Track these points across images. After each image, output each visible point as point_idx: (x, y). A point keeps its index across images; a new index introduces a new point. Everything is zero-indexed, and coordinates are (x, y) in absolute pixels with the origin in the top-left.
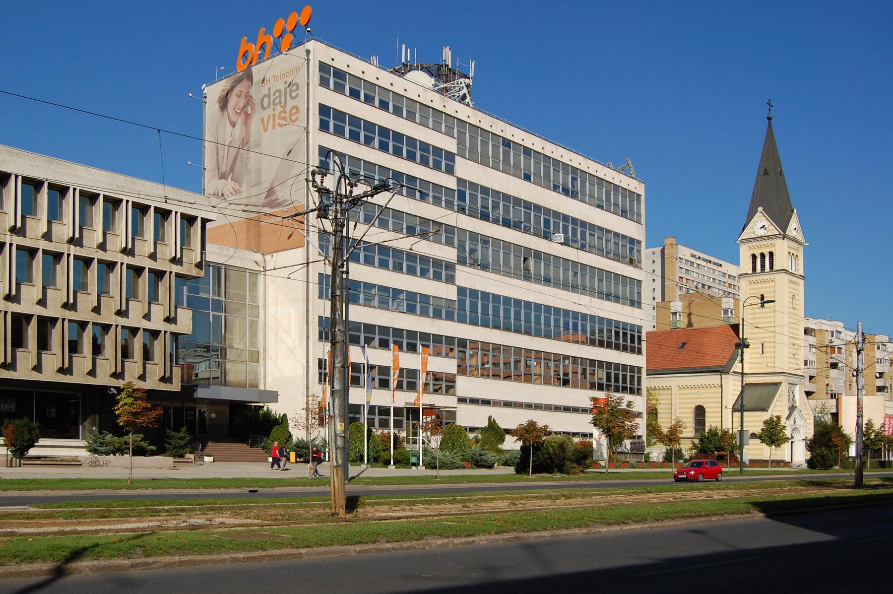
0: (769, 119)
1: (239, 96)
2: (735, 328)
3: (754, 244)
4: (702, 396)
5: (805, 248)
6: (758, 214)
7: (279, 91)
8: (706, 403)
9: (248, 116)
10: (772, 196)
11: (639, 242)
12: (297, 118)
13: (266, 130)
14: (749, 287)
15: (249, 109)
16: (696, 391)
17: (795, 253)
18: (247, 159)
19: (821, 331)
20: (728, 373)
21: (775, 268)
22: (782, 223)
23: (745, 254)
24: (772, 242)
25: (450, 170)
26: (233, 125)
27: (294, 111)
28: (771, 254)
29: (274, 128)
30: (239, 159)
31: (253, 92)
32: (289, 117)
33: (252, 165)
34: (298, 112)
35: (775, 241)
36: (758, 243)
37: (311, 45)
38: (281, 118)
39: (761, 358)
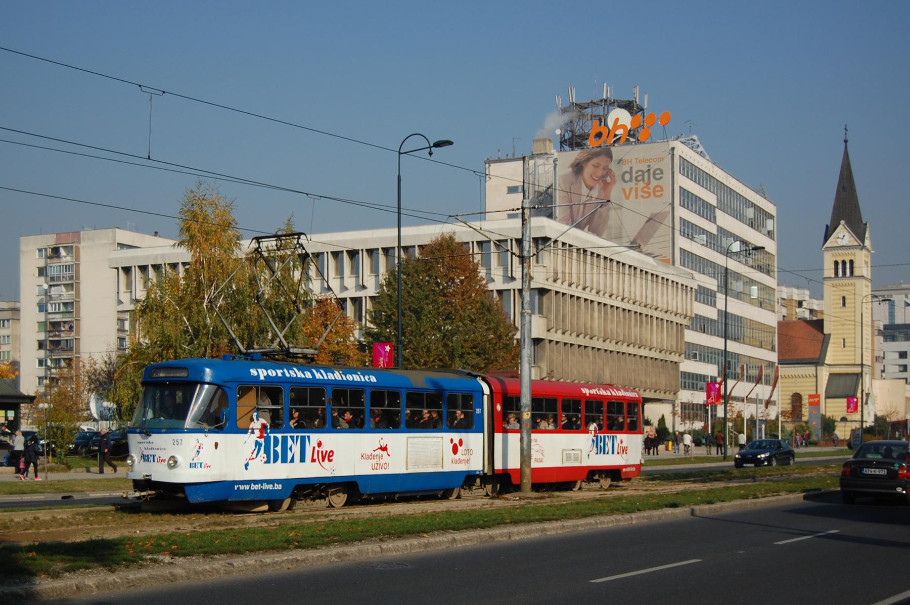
0: (846, 141)
1: (596, 166)
2: (819, 325)
3: (837, 252)
5: (872, 254)
6: (840, 227)
7: (642, 171)
9: (606, 186)
10: (847, 209)
13: (627, 198)
15: (608, 179)
18: (607, 216)
20: (822, 364)
21: (856, 273)
22: (862, 238)
23: (828, 260)
24: (853, 251)
25: (713, 219)
26: (591, 188)
27: (658, 189)
28: (852, 262)
29: (637, 197)
30: (597, 216)
31: (613, 166)
32: (658, 192)
34: (662, 190)
36: (840, 252)
37: (677, 144)
38: (643, 191)
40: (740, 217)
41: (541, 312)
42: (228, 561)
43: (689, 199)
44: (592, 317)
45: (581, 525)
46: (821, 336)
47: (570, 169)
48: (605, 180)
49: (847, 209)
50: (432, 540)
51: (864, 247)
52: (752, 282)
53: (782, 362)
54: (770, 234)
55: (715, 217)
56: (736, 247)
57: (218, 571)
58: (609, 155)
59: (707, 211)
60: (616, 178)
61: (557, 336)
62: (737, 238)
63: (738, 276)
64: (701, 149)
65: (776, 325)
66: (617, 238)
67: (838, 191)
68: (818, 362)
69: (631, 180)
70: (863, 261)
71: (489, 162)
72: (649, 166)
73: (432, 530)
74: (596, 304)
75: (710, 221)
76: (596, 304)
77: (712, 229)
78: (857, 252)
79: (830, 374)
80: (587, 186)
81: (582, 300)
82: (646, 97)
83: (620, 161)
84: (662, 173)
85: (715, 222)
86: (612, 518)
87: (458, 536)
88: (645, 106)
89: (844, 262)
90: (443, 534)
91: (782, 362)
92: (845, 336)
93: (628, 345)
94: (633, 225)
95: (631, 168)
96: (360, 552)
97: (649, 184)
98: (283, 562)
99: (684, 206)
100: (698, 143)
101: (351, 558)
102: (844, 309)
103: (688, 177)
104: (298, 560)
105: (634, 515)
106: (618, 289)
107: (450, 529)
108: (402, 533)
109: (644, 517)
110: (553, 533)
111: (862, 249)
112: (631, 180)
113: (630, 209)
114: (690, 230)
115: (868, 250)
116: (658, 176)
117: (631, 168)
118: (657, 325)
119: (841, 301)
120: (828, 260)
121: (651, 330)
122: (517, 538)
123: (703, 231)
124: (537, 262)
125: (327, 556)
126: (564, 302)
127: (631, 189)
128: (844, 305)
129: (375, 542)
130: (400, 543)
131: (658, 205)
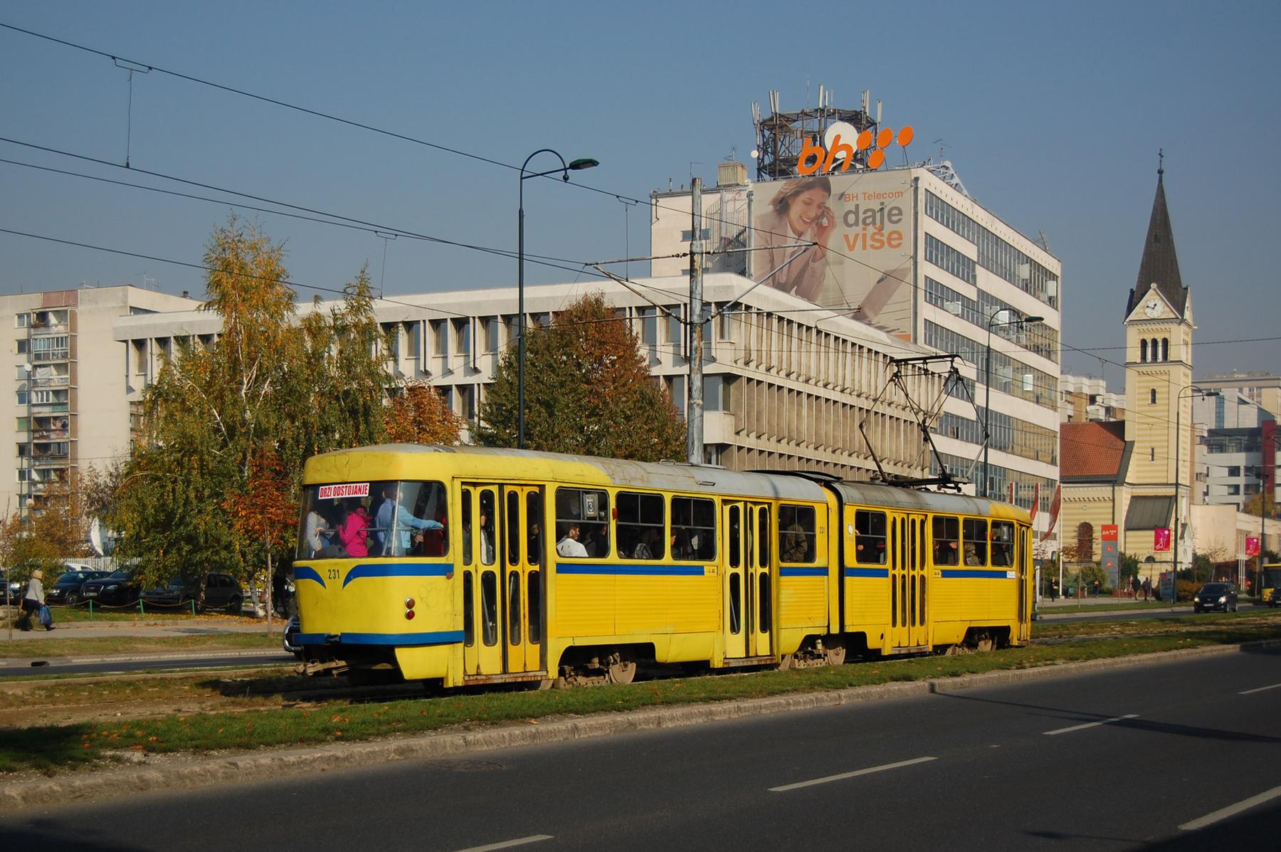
0: (1160, 172)
3: (1145, 327)
6: (1151, 291)
7: (873, 211)
9: (822, 230)
10: (1160, 268)
12: (899, 245)
13: (851, 248)
15: (825, 222)
16: (1082, 505)
18: (823, 274)
20: (1122, 483)
21: (1172, 357)
22: (1180, 309)
23: (1133, 338)
24: (1167, 326)
28: (1165, 341)
29: (864, 247)
31: (831, 203)
33: (829, 281)
34: (900, 237)
35: (1170, 326)
36: (1150, 327)
40: (1009, 276)
41: (726, 407)
42: (230, 760)
43: (937, 251)
44: (799, 415)
45: (766, 707)
46: (1120, 444)
47: (771, 208)
48: (821, 223)
49: (1160, 268)
50: (542, 728)
51: (1183, 321)
52: (1026, 368)
53: (1064, 480)
54: (1051, 301)
55: (974, 277)
56: (1004, 317)
57: (213, 774)
58: (827, 188)
59: (964, 268)
60: (837, 220)
61: (750, 441)
62: (1006, 307)
63: (1006, 360)
64: (956, 180)
65: (1058, 429)
66: (837, 306)
67: (1148, 242)
68: (1115, 480)
69: (856, 223)
70: (1180, 339)
71: (656, 196)
72: (882, 204)
73: (544, 714)
74: (804, 397)
75: (968, 281)
76: (804, 397)
77: (971, 293)
78: (1174, 327)
79: (1133, 497)
80: (794, 231)
81: (786, 391)
82: (880, 106)
83: (842, 195)
84: (900, 213)
85: (974, 284)
86: (811, 696)
87: (582, 722)
88: (879, 120)
89: (1155, 342)
90: (560, 720)
91: (1064, 480)
92: (1153, 445)
93: (850, 455)
94: (857, 287)
95: (857, 206)
96: (433, 746)
97: (881, 229)
98: (314, 760)
99: (930, 261)
100: (952, 171)
101: (420, 754)
102: (1154, 407)
103: (936, 219)
104: (337, 758)
105: (843, 693)
106: (836, 375)
107: (570, 712)
108: (499, 718)
109: (858, 696)
110: (725, 717)
111: (1180, 324)
112: (856, 223)
113: (853, 266)
114: (938, 294)
115: (1188, 325)
116: (895, 219)
117: (857, 206)
118: (891, 427)
119: (1150, 396)
120: (1133, 338)
121: (883, 434)
122: (670, 725)
123: (957, 296)
124: (722, 336)
125: (382, 752)
126: (760, 394)
127: (857, 236)
128: (1154, 401)
129: (457, 731)
130: (494, 733)
131: (893, 259)
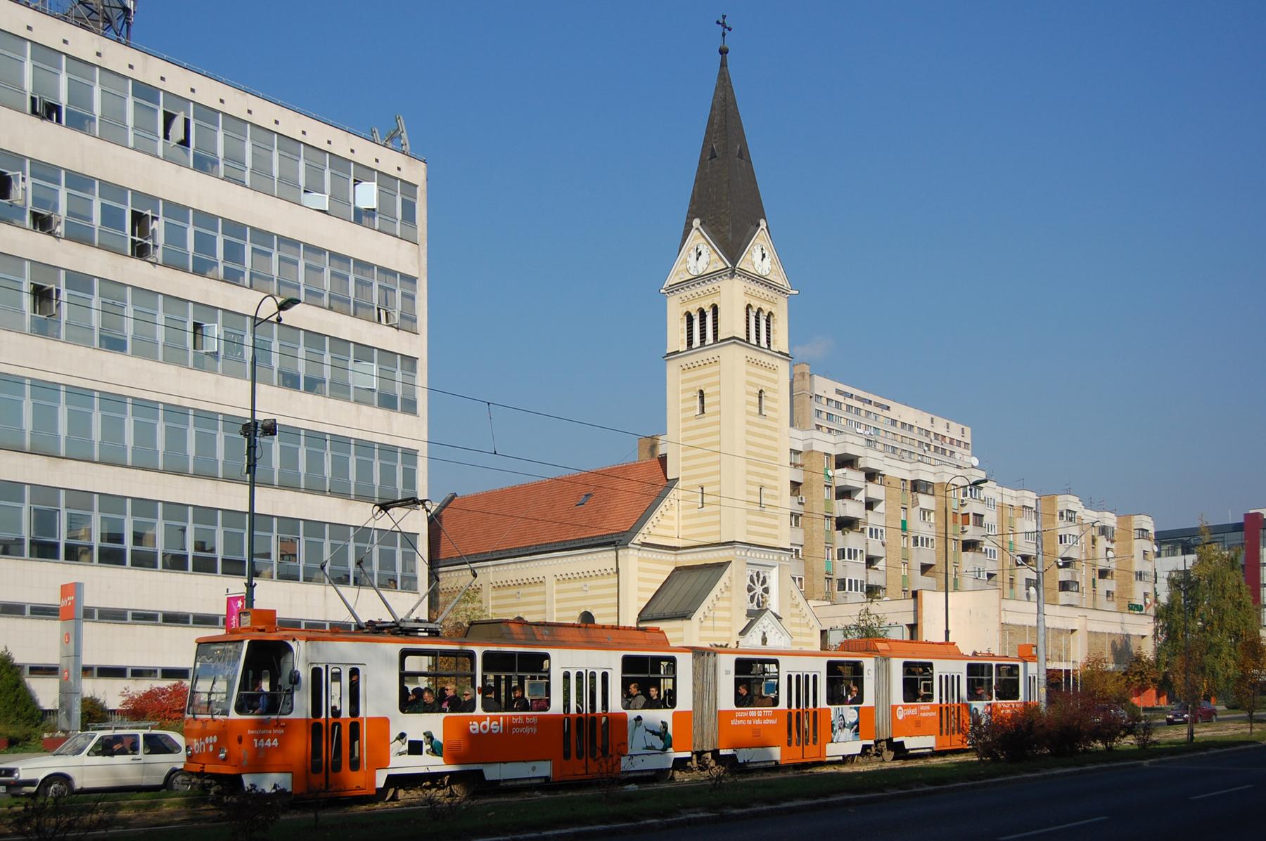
3: (688, 292)
4: (590, 593)
5: (791, 299)
6: (694, 234)
8: (596, 607)
10: (727, 204)
11: (412, 280)
14: (682, 377)
17: (767, 308)
19: (945, 486)
21: (720, 337)
22: (732, 247)
23: (675, 311)
39: (699, 515)
78: (725, 284)
92: (702, 481)
